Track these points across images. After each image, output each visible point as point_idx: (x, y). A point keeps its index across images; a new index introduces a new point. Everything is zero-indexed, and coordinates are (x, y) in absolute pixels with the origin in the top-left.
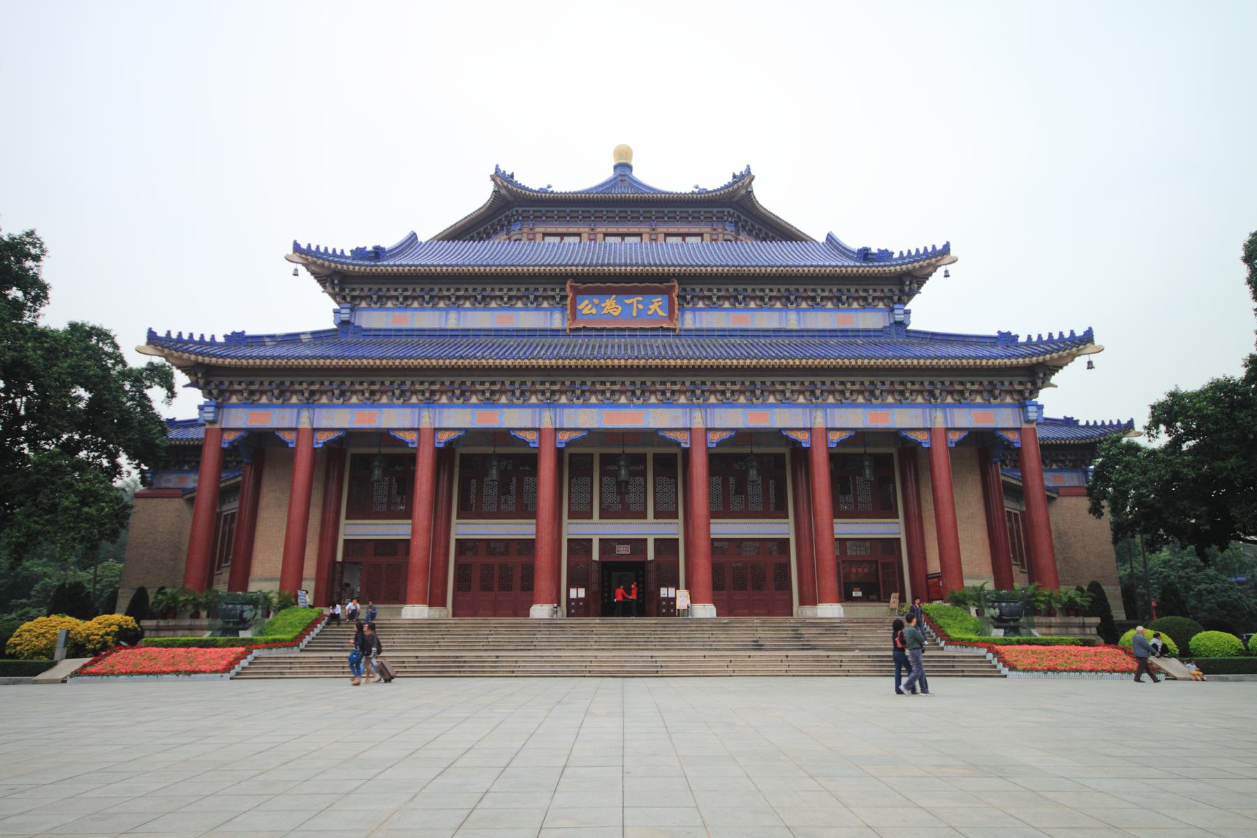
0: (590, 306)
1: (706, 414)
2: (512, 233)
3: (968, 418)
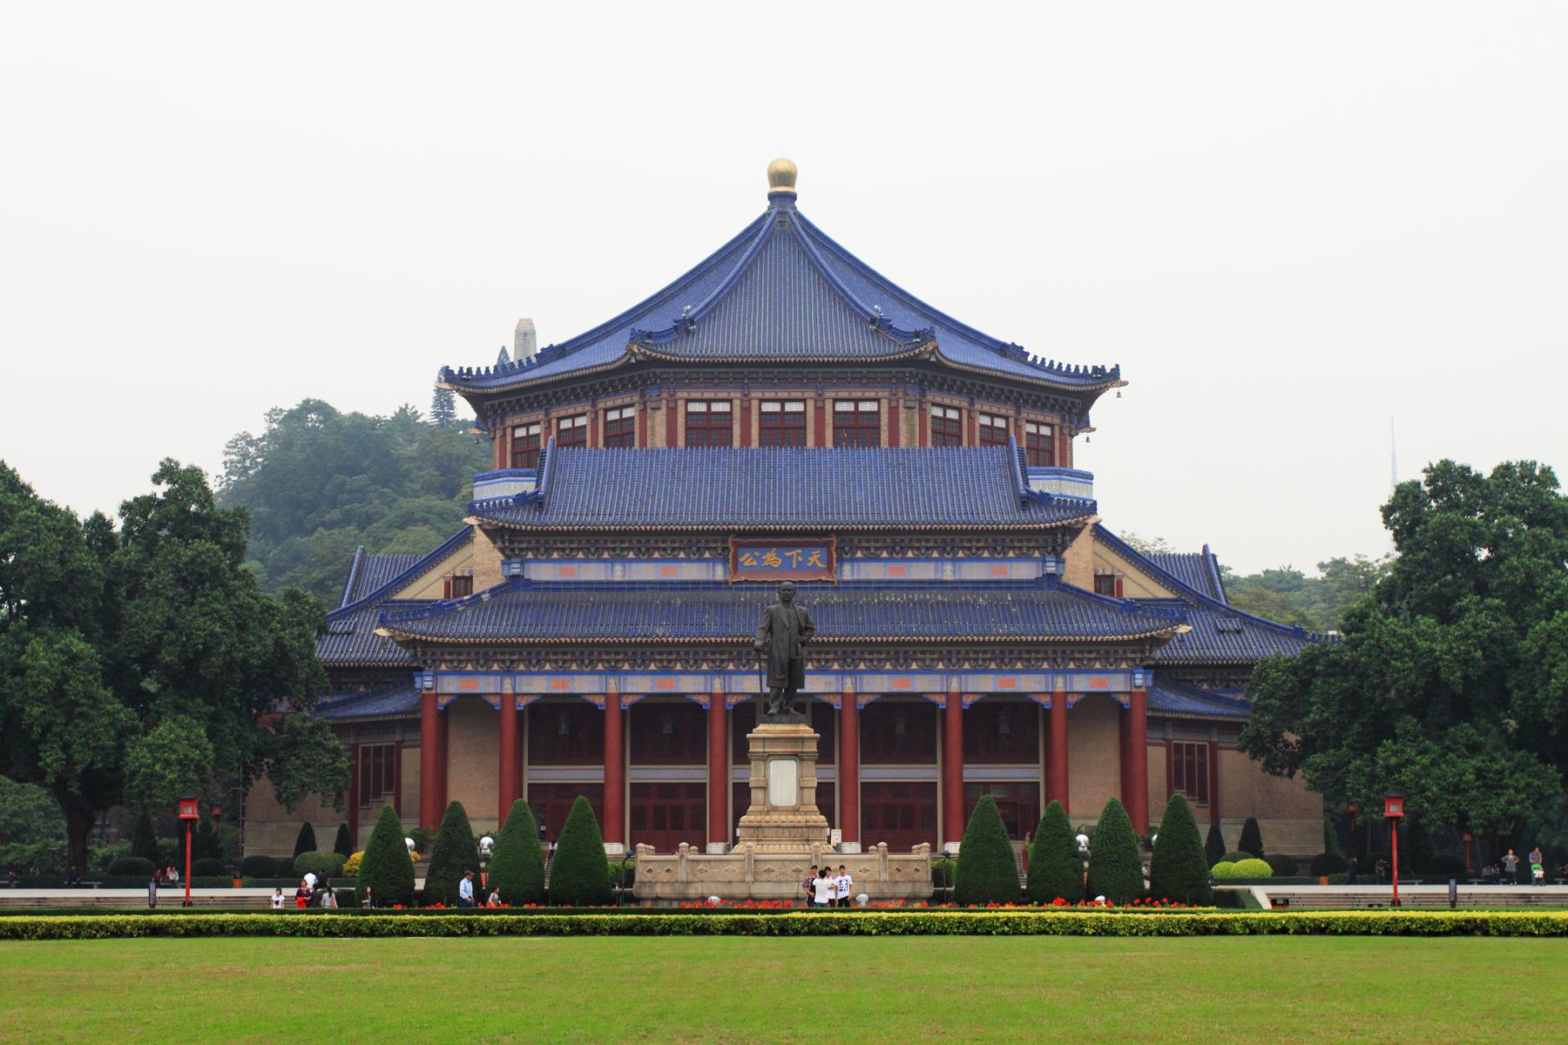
2: (647, 397)
3: (1082, 684)
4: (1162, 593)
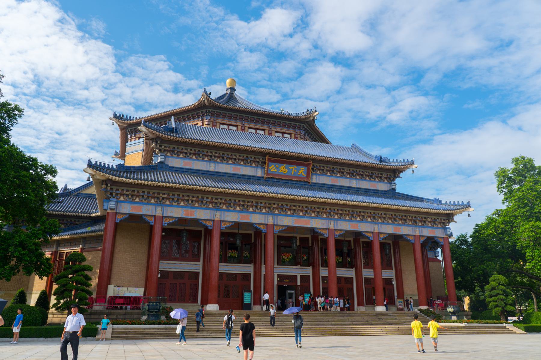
0: (274, 168)
1: (335, 222)
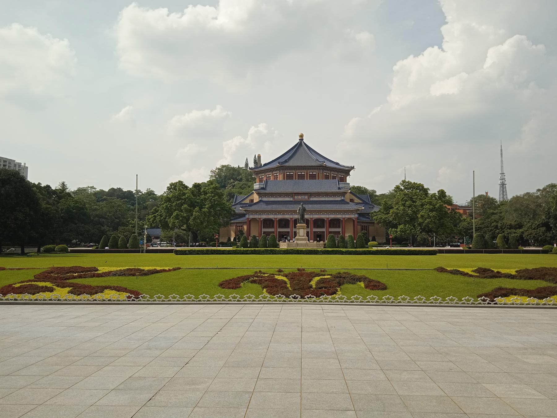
3: (347, 216)
4: (361, 202)
